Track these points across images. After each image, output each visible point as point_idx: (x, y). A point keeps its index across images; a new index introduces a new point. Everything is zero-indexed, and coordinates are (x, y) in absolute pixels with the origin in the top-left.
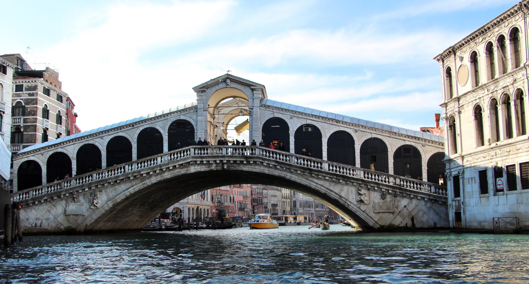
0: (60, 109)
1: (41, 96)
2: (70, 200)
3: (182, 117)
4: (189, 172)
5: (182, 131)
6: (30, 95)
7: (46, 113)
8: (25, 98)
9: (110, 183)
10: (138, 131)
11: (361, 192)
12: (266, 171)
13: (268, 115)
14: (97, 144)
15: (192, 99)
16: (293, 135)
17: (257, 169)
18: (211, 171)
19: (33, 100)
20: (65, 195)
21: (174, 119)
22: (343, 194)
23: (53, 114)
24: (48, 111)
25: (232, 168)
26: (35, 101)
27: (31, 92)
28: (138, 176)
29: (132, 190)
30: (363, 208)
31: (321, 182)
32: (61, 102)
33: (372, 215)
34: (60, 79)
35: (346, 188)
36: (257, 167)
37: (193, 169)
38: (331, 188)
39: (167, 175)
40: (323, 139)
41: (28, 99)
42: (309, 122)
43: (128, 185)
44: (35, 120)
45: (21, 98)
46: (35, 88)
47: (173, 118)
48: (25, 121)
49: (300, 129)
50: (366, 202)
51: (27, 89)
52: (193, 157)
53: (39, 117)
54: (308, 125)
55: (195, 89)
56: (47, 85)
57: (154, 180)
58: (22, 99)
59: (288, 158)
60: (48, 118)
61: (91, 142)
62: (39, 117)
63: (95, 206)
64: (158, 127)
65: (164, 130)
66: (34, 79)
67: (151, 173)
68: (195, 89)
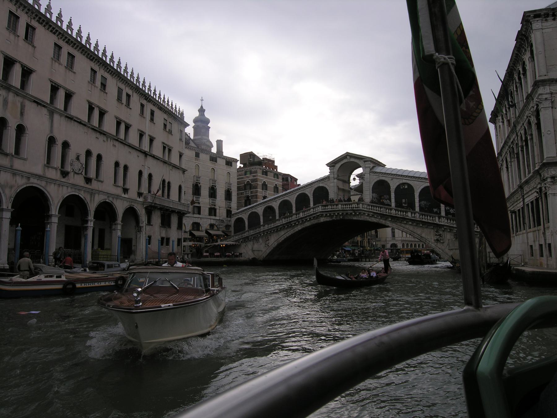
0: (276, 183)
2: (255, 241)
3: (321, 185)
4: (320, 222)
6: (254, 176)
7: (265, 186)
10: (296, 196)
12: (368, 219)
13: (375, 179)
14: (273, 206)
15: (326, 172)
17: (362, 218)
18: (334, 220)
21: (316, 186)
22: (423, 235)
23: (271, 186)
24: (266, 185)
25: (346, 218)
26: (255, 180)
28: (289, 225)
29: (288, 235)
30: (439, 245)
31: (407, 226)
32: (278, 178)
33: (447, 250)
34: (276, 164)
35: (426, 230)
36: (362, 217)
37: (322, 220)
38: (415, 231)
39: (307, 224)
42: (404, 181)
43: (286, 231)
44: (257, 192)
46: (256, 172)
47: (316, 186)
48: (251, 193)
49: (398, 187)
50: (442, 241)
53: (259, 190)
54: (404, 184)
55: (328, 165)
57: (299, 228)
60: (266, 190)
61: (270, 205)
62: (259, 190)
64: (307, 193)
66: (255, 167)
68: (328, 165)
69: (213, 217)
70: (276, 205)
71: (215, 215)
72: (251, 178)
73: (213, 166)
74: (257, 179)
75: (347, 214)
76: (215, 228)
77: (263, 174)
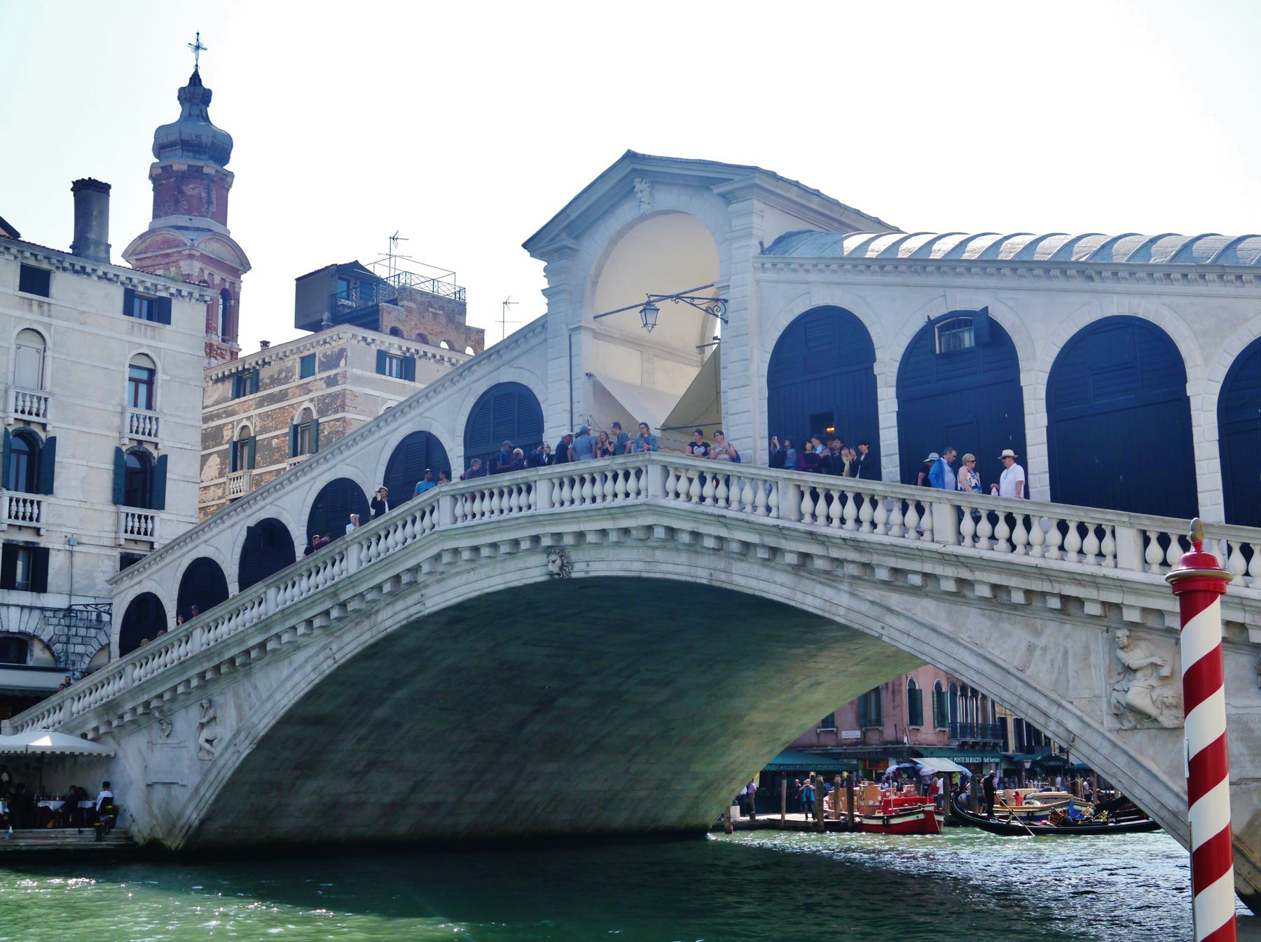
1: (359, 380)
2: (156, 726)
3: (506, 376)
5: (507, 429)
6: (331, 382)
8: (319, 393)
9: (232, 661)
11: (1137, 656)
16: (893, 379)
19: (334, 397)
20: (134, 709)
21: (481, 388)
22: (1040, 672)
27: (332, 373)
34: (471, 320)
39: (390, 618)
40: (1024, 380)
41: (324, 397)
45: (311, 395)
51: (326, 366)
52: (445, 535)
54: (956, 321)
56: (395, 346)
58: (311, 400)
59: (773, 500)
63: (208, 752)
65: (452, 432)
67: (335, 614)
69: (27, 598)
70: (294, 510)
71: (38, 582)
72: (321, 390)
73: (33, 318)
74: (342, 394)
75: (581, 535)
76: (38, 654)
77: (380, 369)
